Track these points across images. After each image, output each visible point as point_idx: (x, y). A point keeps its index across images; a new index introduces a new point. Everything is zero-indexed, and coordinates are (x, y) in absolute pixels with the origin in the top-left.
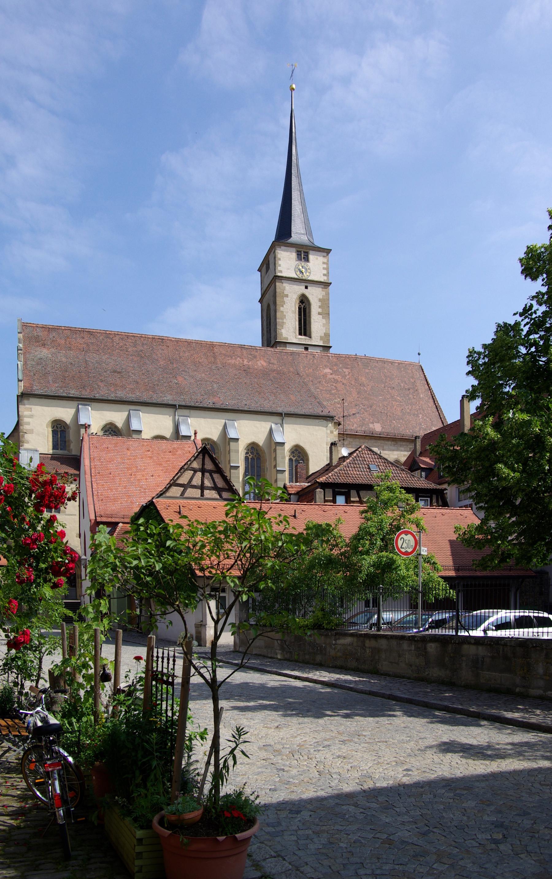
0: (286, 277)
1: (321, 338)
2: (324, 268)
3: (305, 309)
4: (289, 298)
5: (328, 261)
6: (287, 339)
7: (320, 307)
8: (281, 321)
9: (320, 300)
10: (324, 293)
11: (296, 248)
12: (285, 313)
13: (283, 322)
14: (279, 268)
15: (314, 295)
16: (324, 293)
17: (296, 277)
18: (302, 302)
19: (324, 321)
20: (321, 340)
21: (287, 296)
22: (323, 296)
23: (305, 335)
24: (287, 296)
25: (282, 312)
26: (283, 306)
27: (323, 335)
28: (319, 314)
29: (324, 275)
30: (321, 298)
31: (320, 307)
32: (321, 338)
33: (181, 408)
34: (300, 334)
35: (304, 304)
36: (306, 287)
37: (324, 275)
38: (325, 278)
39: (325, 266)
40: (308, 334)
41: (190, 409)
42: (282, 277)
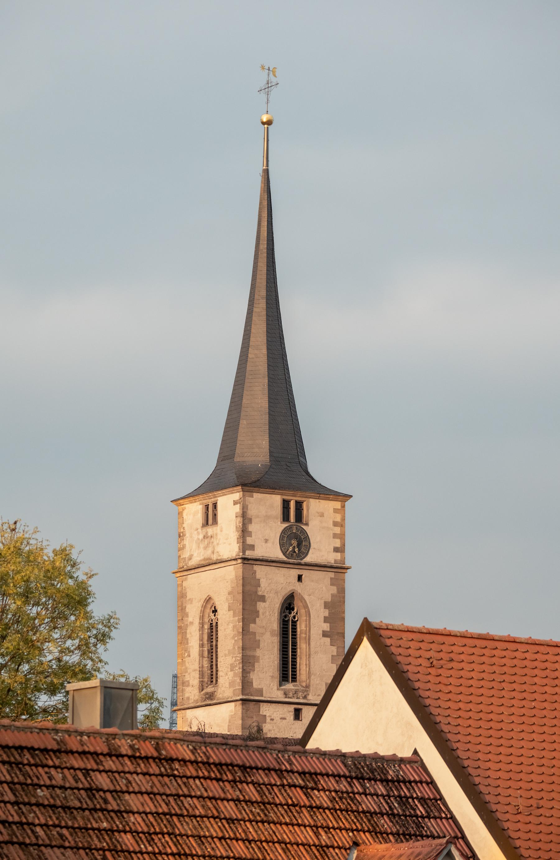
4: (266, 605)
5: (343, 519)
6: (260, 692)
7: (326, 620)
9: (326, 605)
12: (257, 638)
13: (254, 657)
21: (263, 599)
22: (333, 595)
24: (263, 599)
25: (254, 634)
28: (325, 634)
29: (336, 550)
31: (326, 620)
36: (300, 578)
37: (336, 550)
38: (338, 556)
39: (337, 530)
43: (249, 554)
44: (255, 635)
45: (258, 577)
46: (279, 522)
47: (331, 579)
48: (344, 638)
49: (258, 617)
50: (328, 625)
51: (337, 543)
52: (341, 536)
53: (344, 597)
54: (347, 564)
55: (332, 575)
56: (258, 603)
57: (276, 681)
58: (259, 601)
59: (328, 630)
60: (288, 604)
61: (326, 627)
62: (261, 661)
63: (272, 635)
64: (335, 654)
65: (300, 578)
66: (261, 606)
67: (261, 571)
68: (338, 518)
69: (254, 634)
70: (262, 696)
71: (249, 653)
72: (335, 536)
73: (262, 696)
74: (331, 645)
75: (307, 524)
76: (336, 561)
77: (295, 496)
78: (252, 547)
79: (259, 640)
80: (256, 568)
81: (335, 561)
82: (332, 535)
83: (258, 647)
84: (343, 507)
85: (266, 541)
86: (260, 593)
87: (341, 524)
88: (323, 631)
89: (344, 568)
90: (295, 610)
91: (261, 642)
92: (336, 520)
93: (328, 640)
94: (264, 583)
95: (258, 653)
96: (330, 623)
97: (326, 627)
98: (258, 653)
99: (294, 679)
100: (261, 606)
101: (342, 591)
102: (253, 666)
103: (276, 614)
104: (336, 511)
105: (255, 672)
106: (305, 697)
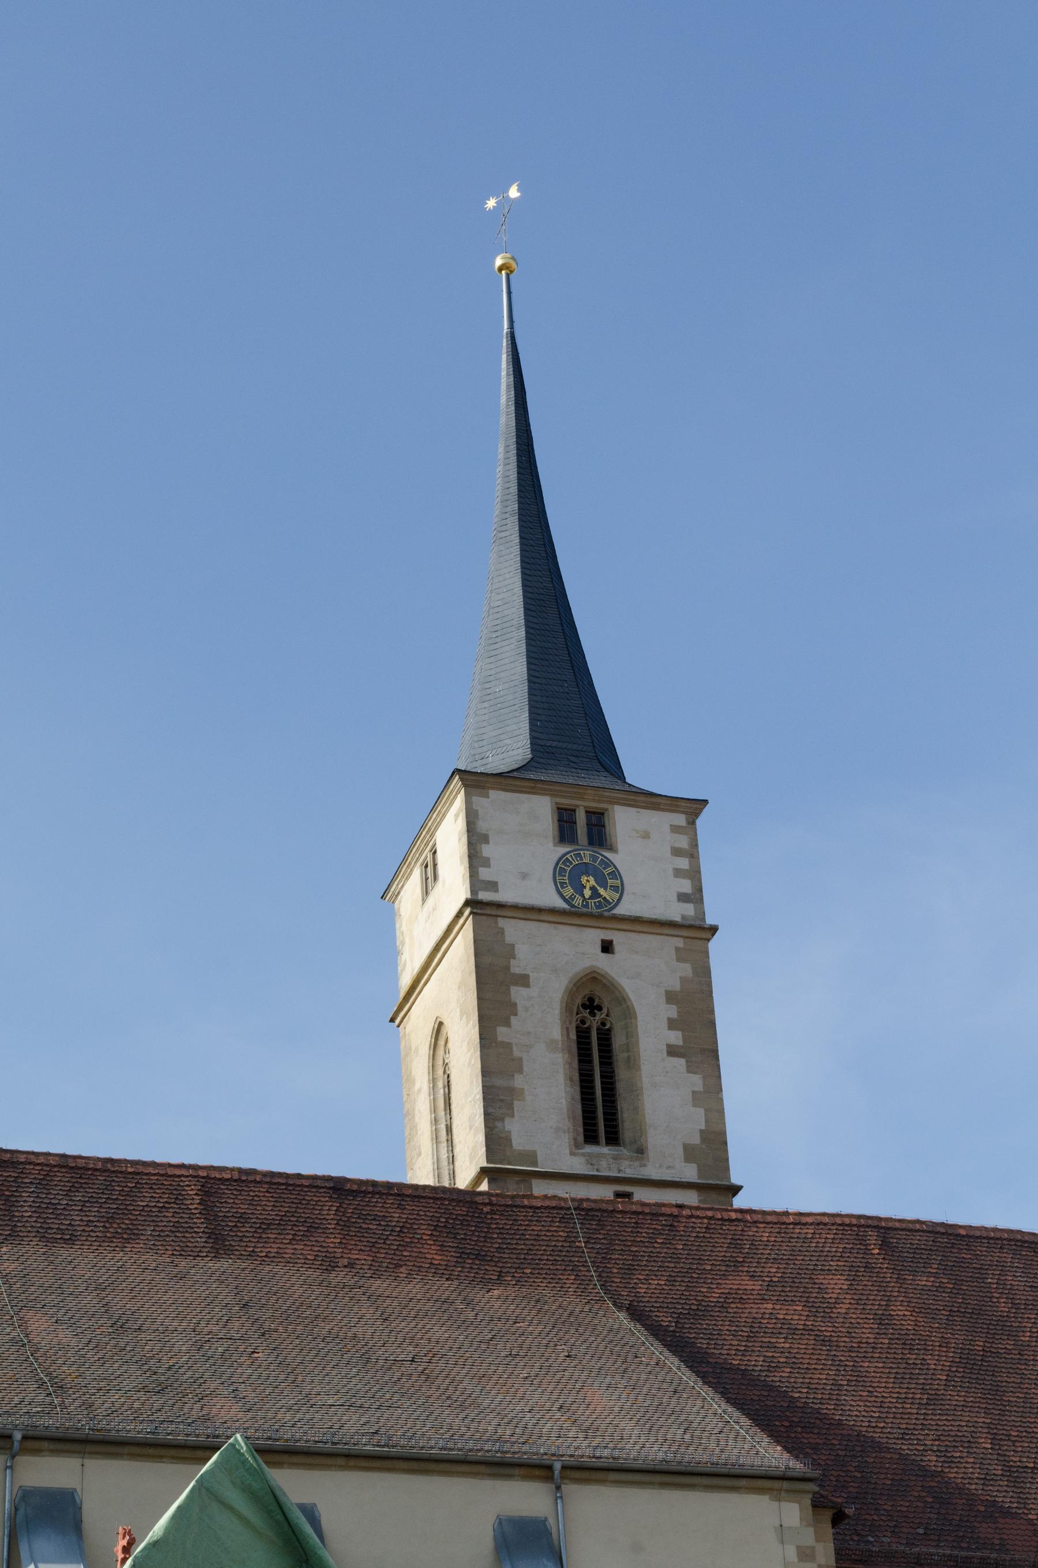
0: (516, 907)
1: (690, 1153)
2: (678, 873)
3: (605, 1037)
4: (533, 991)
5: (694, 844)
6: (531, 1157)
7: (672, 1024)
9: (671, 997)
10: (686, 969)
11: (552, 794)
12: (516, 1053)
15: (643, 974)
16: (686, 969)
17: (560, 904)
18: (591, 1005)
19: (697, 1081)
21: (523, 980)
22: (683, 980)
23: (613, 1138)
24: (523, 980)
25: (508, 1046)
26: (507, 1024)
27: (696, 1140)
28: (672, 1051)
29: (683, 898)
30: (677, 987)
31: (672, 1024)
32: (690, 1153)
33: (37, 1452)
34: (591, 1137)
35: (599, 1016)
36: (607, 947)
37: (683, 898)
38: (689, 909)
39: (684, 863)
40: (627, 1131)
41: (83, 1454)
42: (500, 906)
43: (484, 896)
44: (511, 1048)
45: (509, 939)
46: (551, 844)
47: (677, 949)
48: (716, 1057)
49: (516, 1014)
50: (679, 1034)
51: (686, 886)
52: (694, 874)
53: (709, 984)
54: (710, 921)
55: (680, 943)
56: (514, 990)
58: (516, 984)
59: (681, 1043)
61: (675, 1037)
62: (529, 1098)
63: (551, 1045)
64: (699, 1087)
65: (607, 947)
66: (518, 994)
67: (513, 930)
68: (683, 842)
70: (535, 1164)
71: (499, 1082)
72: (678, 873)
73: (535, 1164)
74: (689, 1071)
75: (612, 849)
76: (683, 917)
77: (583, 799)
78: (493, 886)
79: (521, 1059)
80: (502, 922)
81: (683, 917)
82: (671, 872)
83: (520, 1070)
84: (693, 823)
85: (524, 876)
87: (692, 853)
88: (669, 1046)
89: (701, 928)
90: (605, 1010)
91: (525, 1063)
92: (677, 845)
93: (681, 1062)
94: (522, 951)
95: (518, 1081)
96: (683, 1031)
97: (675, 1037)
98: (518, 1081)
100: (518, 994)
101: (703, 972)
102: (511, 1107)
103: (557, 1012)
104: (675, 829)
105: (516, 1118)
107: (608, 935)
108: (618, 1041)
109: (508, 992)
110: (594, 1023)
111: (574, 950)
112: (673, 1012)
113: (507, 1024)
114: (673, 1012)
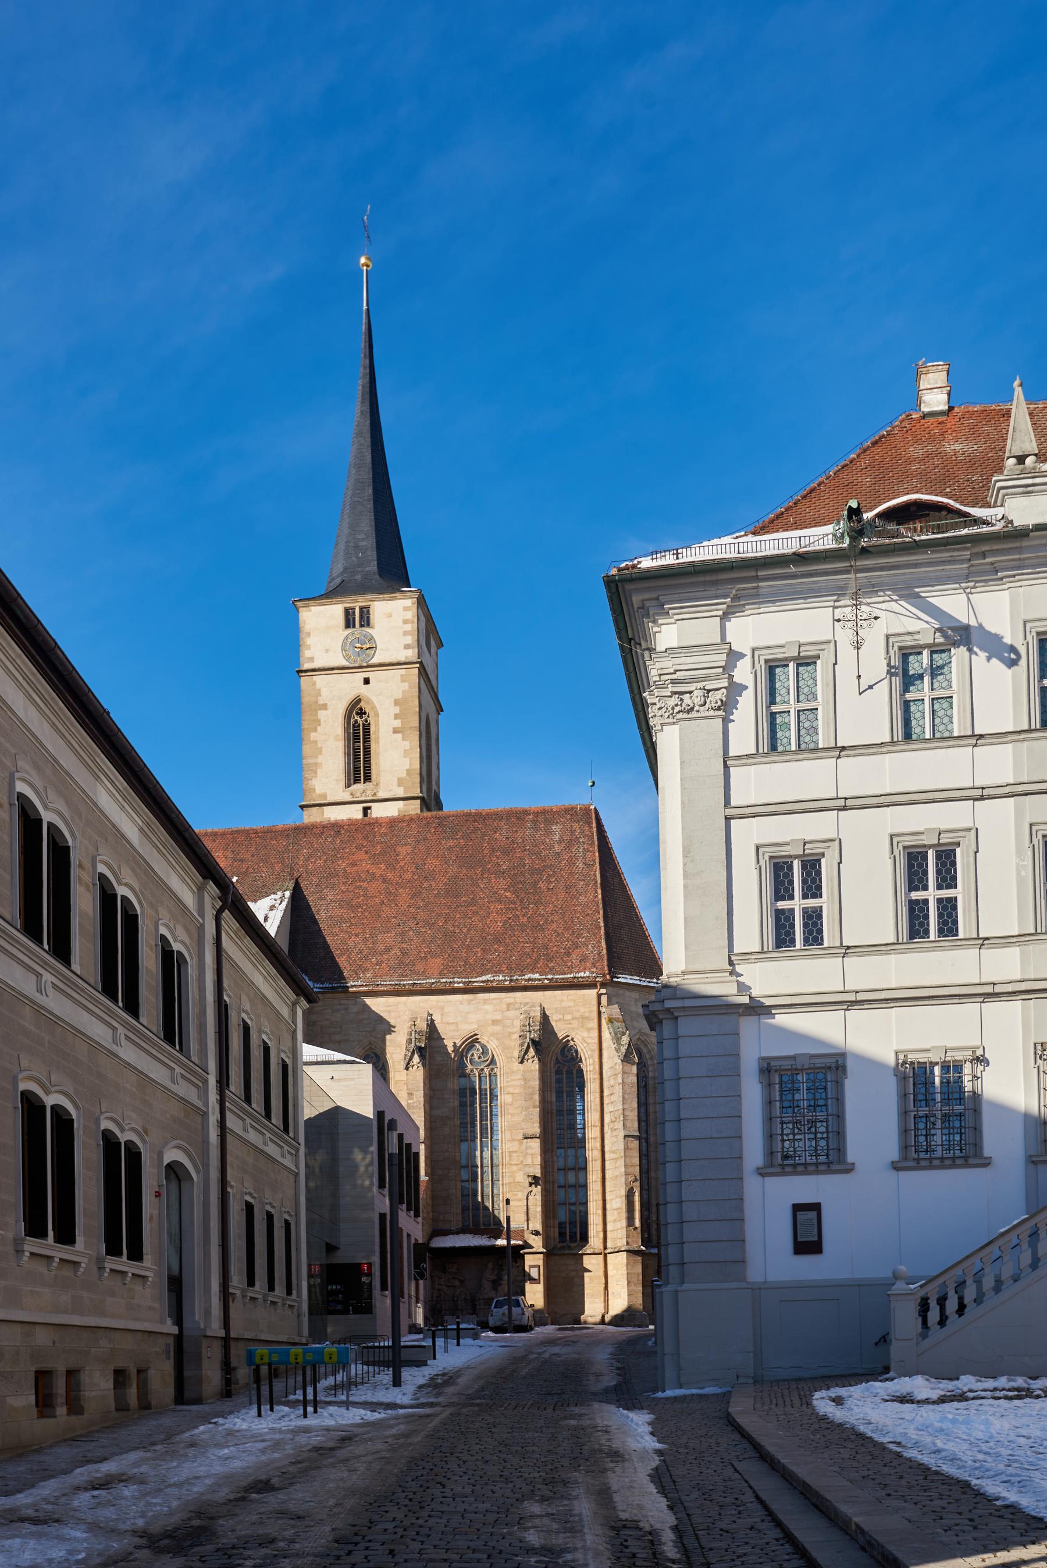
4: (329, 712)
7: (396, 717)
8: (311, 761)
9: (397, 702)
12: (319, 745)
13: (316, 764)
14: (307, 653)
20: (399, 785)
25: (315, 742)
26: (315, 730)
28: (396, 731)
31: (396, 717)
36: (367, 681)
50: (399, 721)
57: (342, 783)
60: (356, 709)
61: (397, 723)
64: (408, 748)
65: (367, 681)
66: (322, 714)
69: (315, 742)
83: (321, 753)
86: (321, 702)
93: (400, 735)
97: (397, 723)
99: (368, 778)
102: (316, 772)
106: (375, 794)
107: (366, 675)
108: (372, 729)
109: (316, 714)
110: (360, 721)
111: (349, 686)
112: (397, 710)
113: (315, 730)
114: (397, 710)
